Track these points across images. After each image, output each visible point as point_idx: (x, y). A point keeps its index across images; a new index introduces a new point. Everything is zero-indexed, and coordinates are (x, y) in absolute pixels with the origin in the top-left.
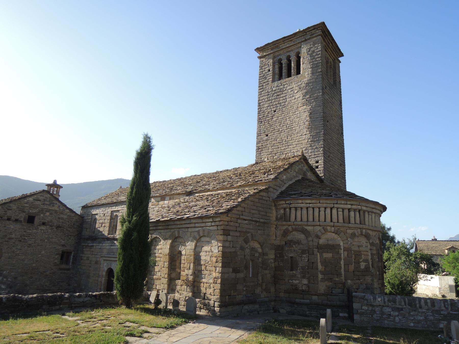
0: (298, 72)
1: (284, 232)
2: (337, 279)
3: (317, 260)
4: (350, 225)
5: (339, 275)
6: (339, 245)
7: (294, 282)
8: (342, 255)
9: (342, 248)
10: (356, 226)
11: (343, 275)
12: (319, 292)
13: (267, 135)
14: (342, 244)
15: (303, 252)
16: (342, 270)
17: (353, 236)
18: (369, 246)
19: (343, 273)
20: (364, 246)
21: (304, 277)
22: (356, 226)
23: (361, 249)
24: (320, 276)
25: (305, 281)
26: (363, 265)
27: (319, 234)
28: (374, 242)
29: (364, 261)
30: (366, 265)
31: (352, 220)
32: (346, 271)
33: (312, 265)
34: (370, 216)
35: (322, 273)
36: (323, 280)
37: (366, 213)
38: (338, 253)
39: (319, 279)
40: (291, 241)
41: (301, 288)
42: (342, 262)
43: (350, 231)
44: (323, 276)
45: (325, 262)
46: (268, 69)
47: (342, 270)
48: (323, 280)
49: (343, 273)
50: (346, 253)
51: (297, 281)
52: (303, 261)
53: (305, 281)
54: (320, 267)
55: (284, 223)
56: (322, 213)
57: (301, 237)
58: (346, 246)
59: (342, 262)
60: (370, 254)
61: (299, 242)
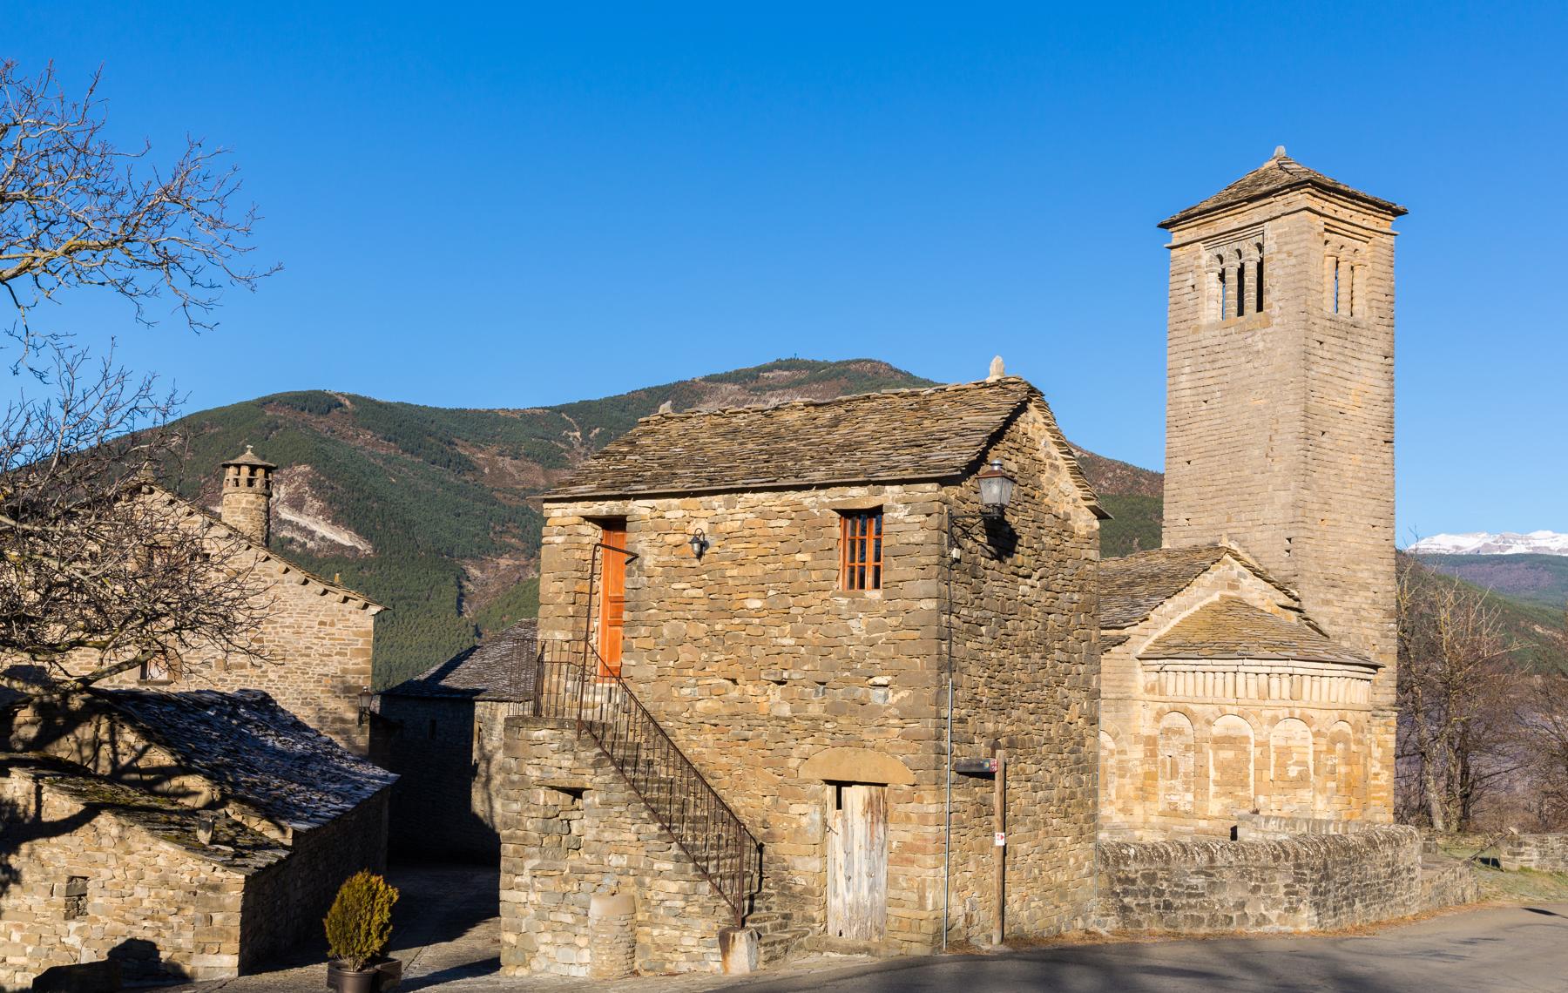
0: (1260, 308)
1: (1158, 713)
2: (1241, 794)
3: (1208, 761)
4: (1268, 702)
5: (1245, 786)
6: (1247, 738)
7: (1172, 797)
8: (1252, 754)
9: (1252, 741)
10: (1281, 703)
11: (1252, 787)
12: (1209, 814)
13: (1189, 462)
14: (1251, 735)
15: (1187, 748)
16: (1251, 779)
17: (1275, 721)
18: (1311, 739)
19: (1252, 784)
20: (1298, 738)
21: (1187, 790)
22: (1281, 703)
23: (1290, 743)
24: (1212, 788)
25: (1189, 797)
26: (1293, 772)
27: (1212, 719)
28: (1323, 730)
29: (1297, 763)
30: (1300, 772)
31: (1275, 693)
32: (1258, 780)
33: (1200, 773)
34: (1316, 685)
35: (1217, 783)
36: (1217, 795)
37: (1307, 680)
38: (1244, 750)
39: (1211, 794)
40: (1168, 730)
41: (1182, 809)
42: (1251, 766)
43: (1268, 714)
44: (1218, 788)
45: (1222, 767)
46: (1190, 282)
47: (1251, 779)
48: (1217, 795)
49: (1252, 784)
50: (1259, 750)
51: (1177, 797)
52: (1187, 764)
53: (1189, 797)
54: (1213, 774)
55: (1157, 697)
56: (1219, 682)
57: (1182, 722)
58: (1260, 739)
59: (1251, 766)
60: (1311, 752)
61: (1180, 732)
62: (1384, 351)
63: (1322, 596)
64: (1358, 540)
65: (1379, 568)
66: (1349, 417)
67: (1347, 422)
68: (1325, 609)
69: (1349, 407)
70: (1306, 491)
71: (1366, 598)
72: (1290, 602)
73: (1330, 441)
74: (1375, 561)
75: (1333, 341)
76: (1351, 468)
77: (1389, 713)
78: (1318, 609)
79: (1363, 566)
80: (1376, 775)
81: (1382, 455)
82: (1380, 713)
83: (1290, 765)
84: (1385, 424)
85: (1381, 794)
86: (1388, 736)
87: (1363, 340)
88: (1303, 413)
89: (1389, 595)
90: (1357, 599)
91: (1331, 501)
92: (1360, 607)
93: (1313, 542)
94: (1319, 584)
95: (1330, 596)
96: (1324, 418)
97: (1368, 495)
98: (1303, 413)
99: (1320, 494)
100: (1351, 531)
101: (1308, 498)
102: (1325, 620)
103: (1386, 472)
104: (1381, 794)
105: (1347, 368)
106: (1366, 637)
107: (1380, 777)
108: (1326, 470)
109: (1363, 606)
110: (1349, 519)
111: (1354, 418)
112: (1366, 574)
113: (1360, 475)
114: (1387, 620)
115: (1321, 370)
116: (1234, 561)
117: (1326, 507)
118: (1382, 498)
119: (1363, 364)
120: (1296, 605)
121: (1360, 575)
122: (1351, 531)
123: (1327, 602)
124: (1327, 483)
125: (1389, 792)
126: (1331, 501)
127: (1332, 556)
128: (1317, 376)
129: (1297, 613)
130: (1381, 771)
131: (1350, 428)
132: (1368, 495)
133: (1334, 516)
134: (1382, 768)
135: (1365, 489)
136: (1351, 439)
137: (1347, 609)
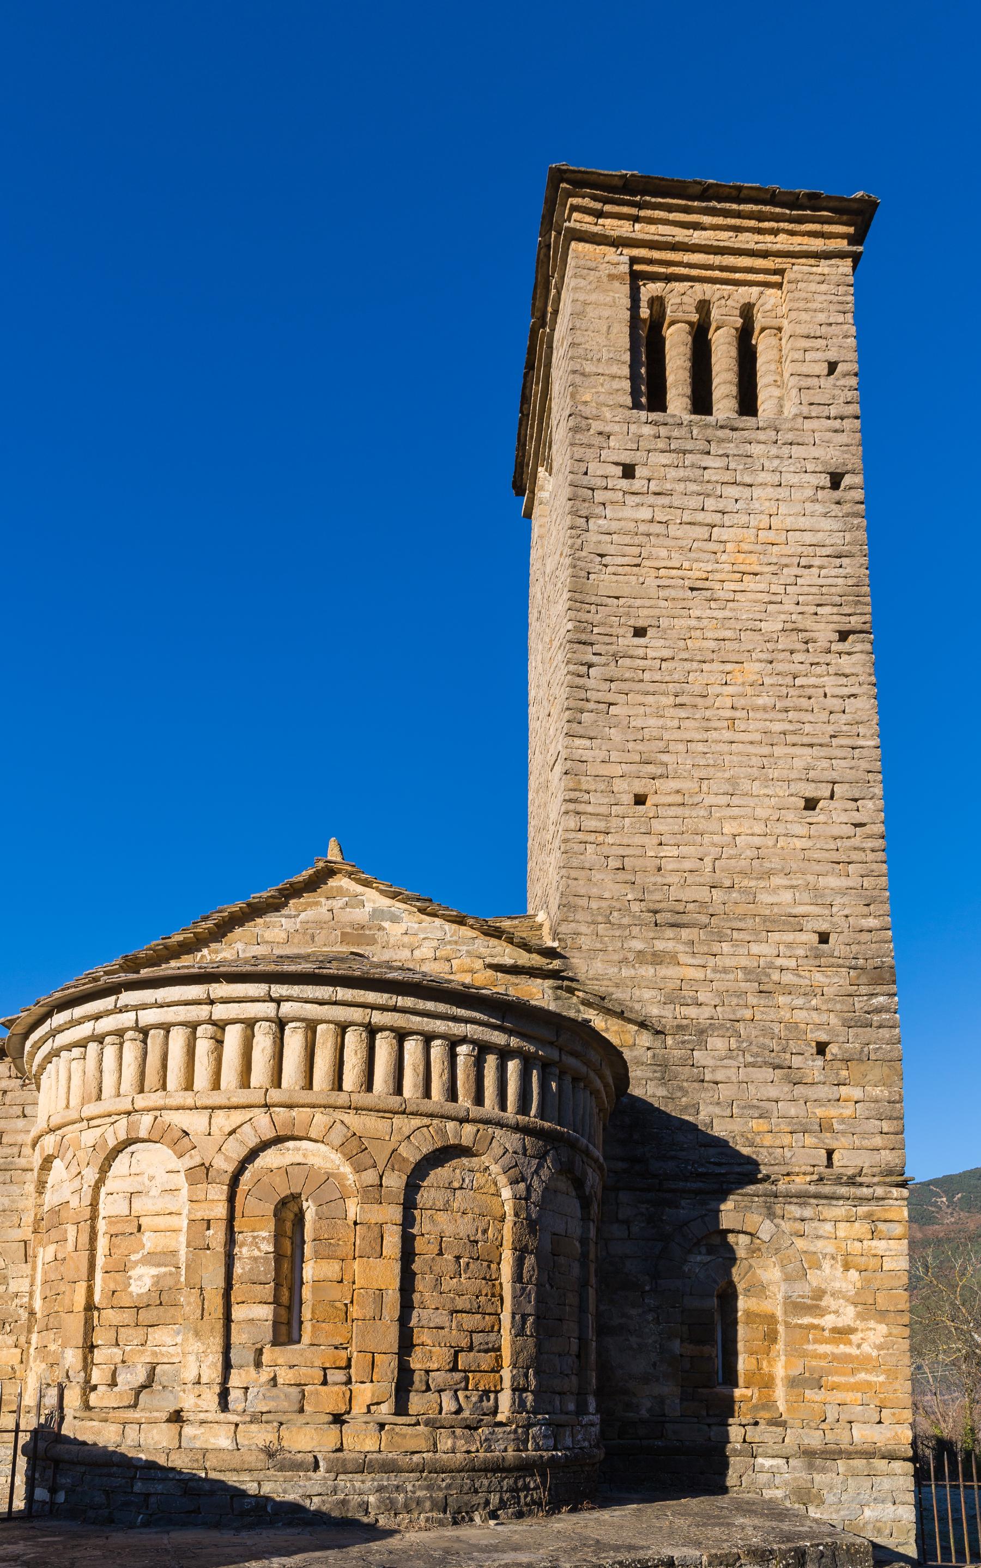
62: (825, 463)
63: (638, 945)
64: (758, 829)
65: (833, 882)
66: (720, 594)
67: (713, 604)
68: (647, 971)
69: (719, 576)
70: (578, 742)
71: (789, 945)
72: (537, 960)
73: (662, 642)
74: (817, 868)
75: (665, 459)
76: (729, 690)
77: (880, 1191)
78: (626, 972)
79: (777, 881)
80: (842, 1333)
81: (829, 659)
82: (843, 1190)
83: (136, 1263)
84: (837, 600)
85: (862, 1376)
86: (880, 1246)
87: (756, 449)
88: (569, 594)
89: (865, 937)
90: (755, 949)
91: (665, 758)
92: (771, 966)
93: (610, 839)
94: (626, 921)
95: (660, 945)
96: (638, 602)
97: (791, 739)
98: (569, 594)
99: (631, 745)
100: (736, 811)
101: (587, 755)
102: (647, 994)
103: (846, 691)
104: (862, 1376)
105: (710, 503)
106: (793, 1026)
107: (855, 1338)
108: (650, 699)
109: (779, 962)
110: (727, 787)
111: (739, 596)
112: (787, 896)
113: (760, 701)
114: (864, 990)
115: (628, 513)
116: (360, 889)
117: (650, 769)
118: (835, 742)
119: (757, 492)
120: (556, 964)
121: (764, 898)
122: (736, 811)
123: (657, 959)
124: (652, 722)
125: (892, 1374)
126: (665, 758)
127: (670, 867)
128: (614, 526)
129: (549, 983)
130: (859, 1324)
131: (720, 614)
132: (791, 739)
133: (673, 784)
134: (859, 1316)
135: (777, 727)
136: (728, 634)
137: (725, 970)
